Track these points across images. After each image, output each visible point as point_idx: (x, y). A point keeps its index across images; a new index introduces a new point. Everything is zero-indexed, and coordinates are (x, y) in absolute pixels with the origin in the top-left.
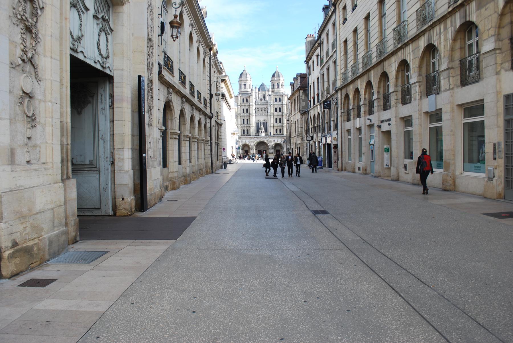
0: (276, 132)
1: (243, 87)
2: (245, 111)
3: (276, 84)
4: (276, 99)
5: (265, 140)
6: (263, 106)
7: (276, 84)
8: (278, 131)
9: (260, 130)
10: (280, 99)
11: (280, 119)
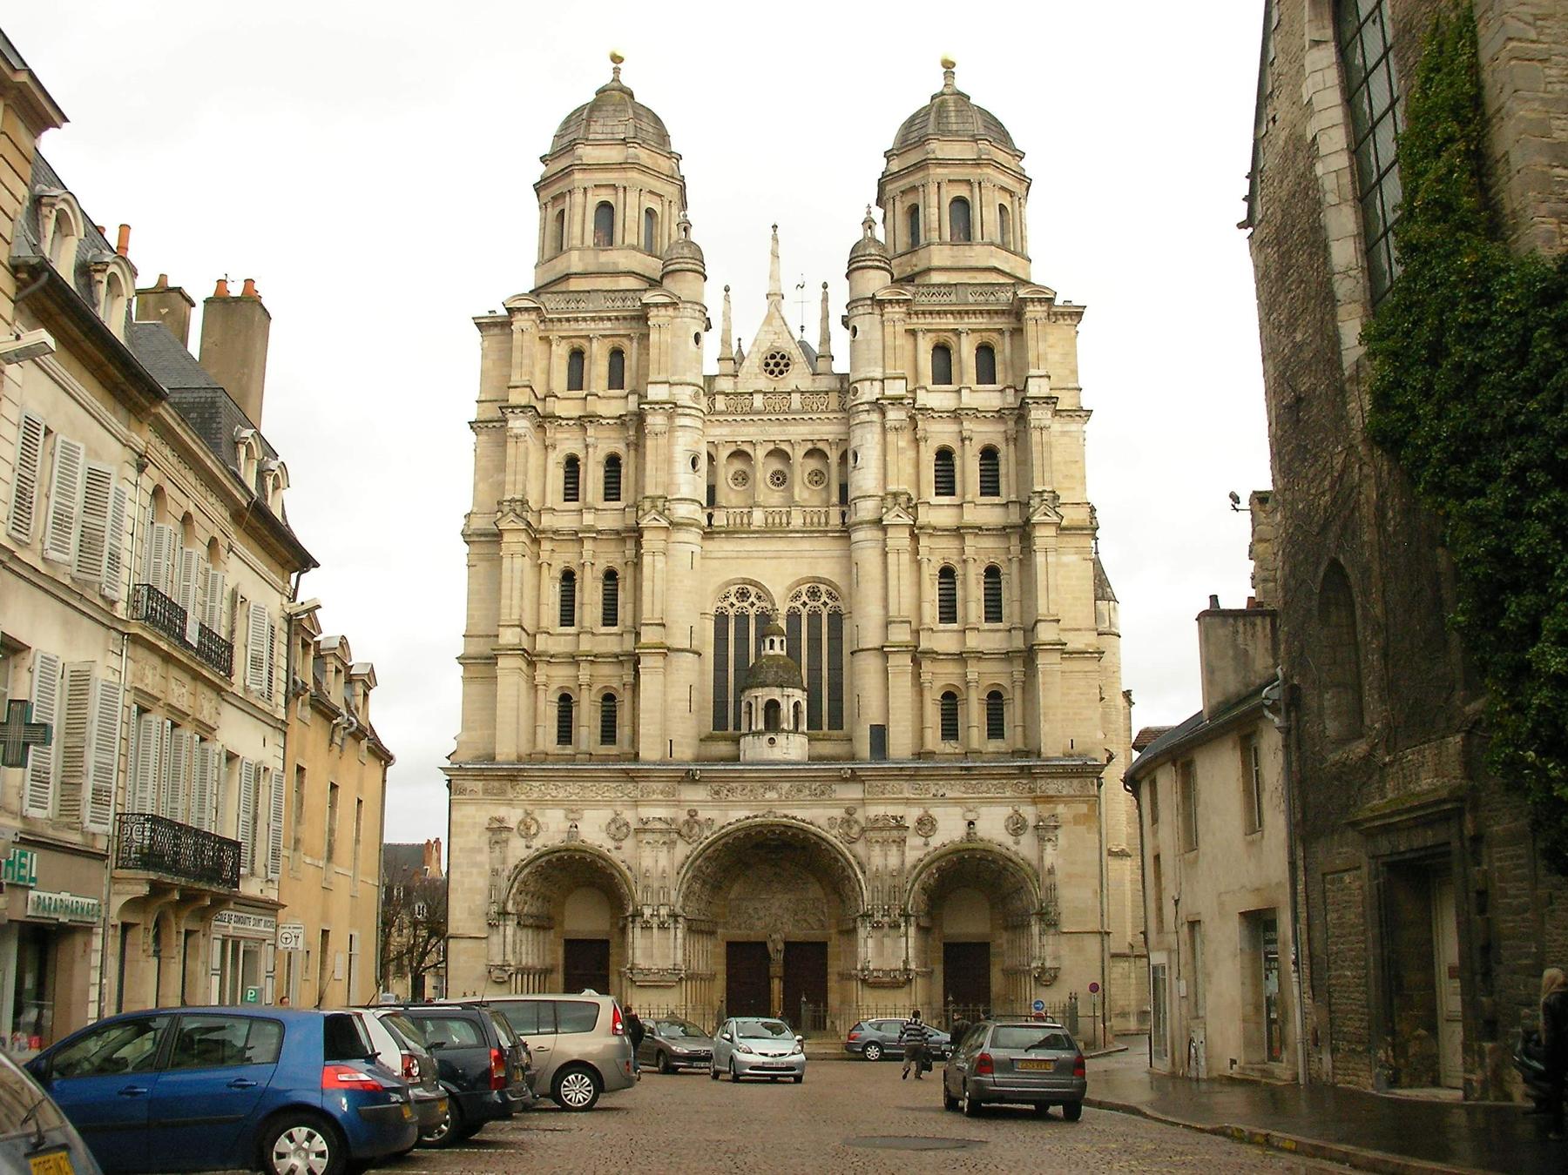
0: (950, 729)
1: (581, 224)
2: (593, 478)
3: (936, 213)
4: (942, 352)
5: (816, 814)
6: (798, 432)
7: (936, 213)
8: (974, 714)
9: (763, 695)
10: (985, 353)
11: (992, 572)
